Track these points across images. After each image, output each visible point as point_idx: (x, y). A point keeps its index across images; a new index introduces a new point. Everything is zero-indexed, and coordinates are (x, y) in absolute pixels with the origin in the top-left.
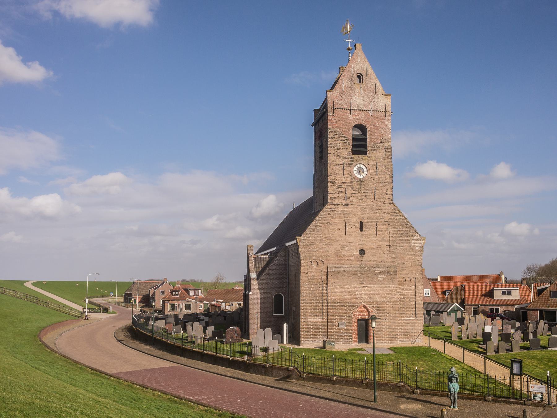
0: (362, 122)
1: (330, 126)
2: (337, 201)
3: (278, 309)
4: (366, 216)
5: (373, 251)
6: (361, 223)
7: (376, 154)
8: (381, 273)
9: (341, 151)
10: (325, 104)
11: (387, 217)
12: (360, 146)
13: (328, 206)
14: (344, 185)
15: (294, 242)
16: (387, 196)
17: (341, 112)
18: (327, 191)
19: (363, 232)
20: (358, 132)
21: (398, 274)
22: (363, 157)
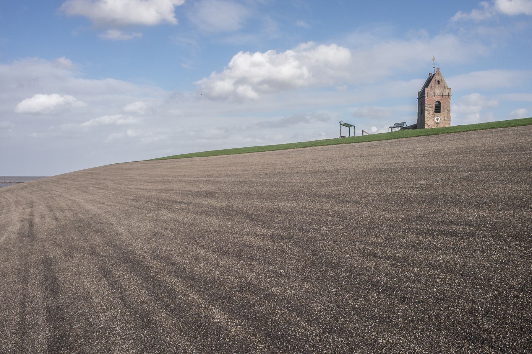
1: (426, 102)
12: (438, 109)
17: (430, 96)
20: (437, 103)
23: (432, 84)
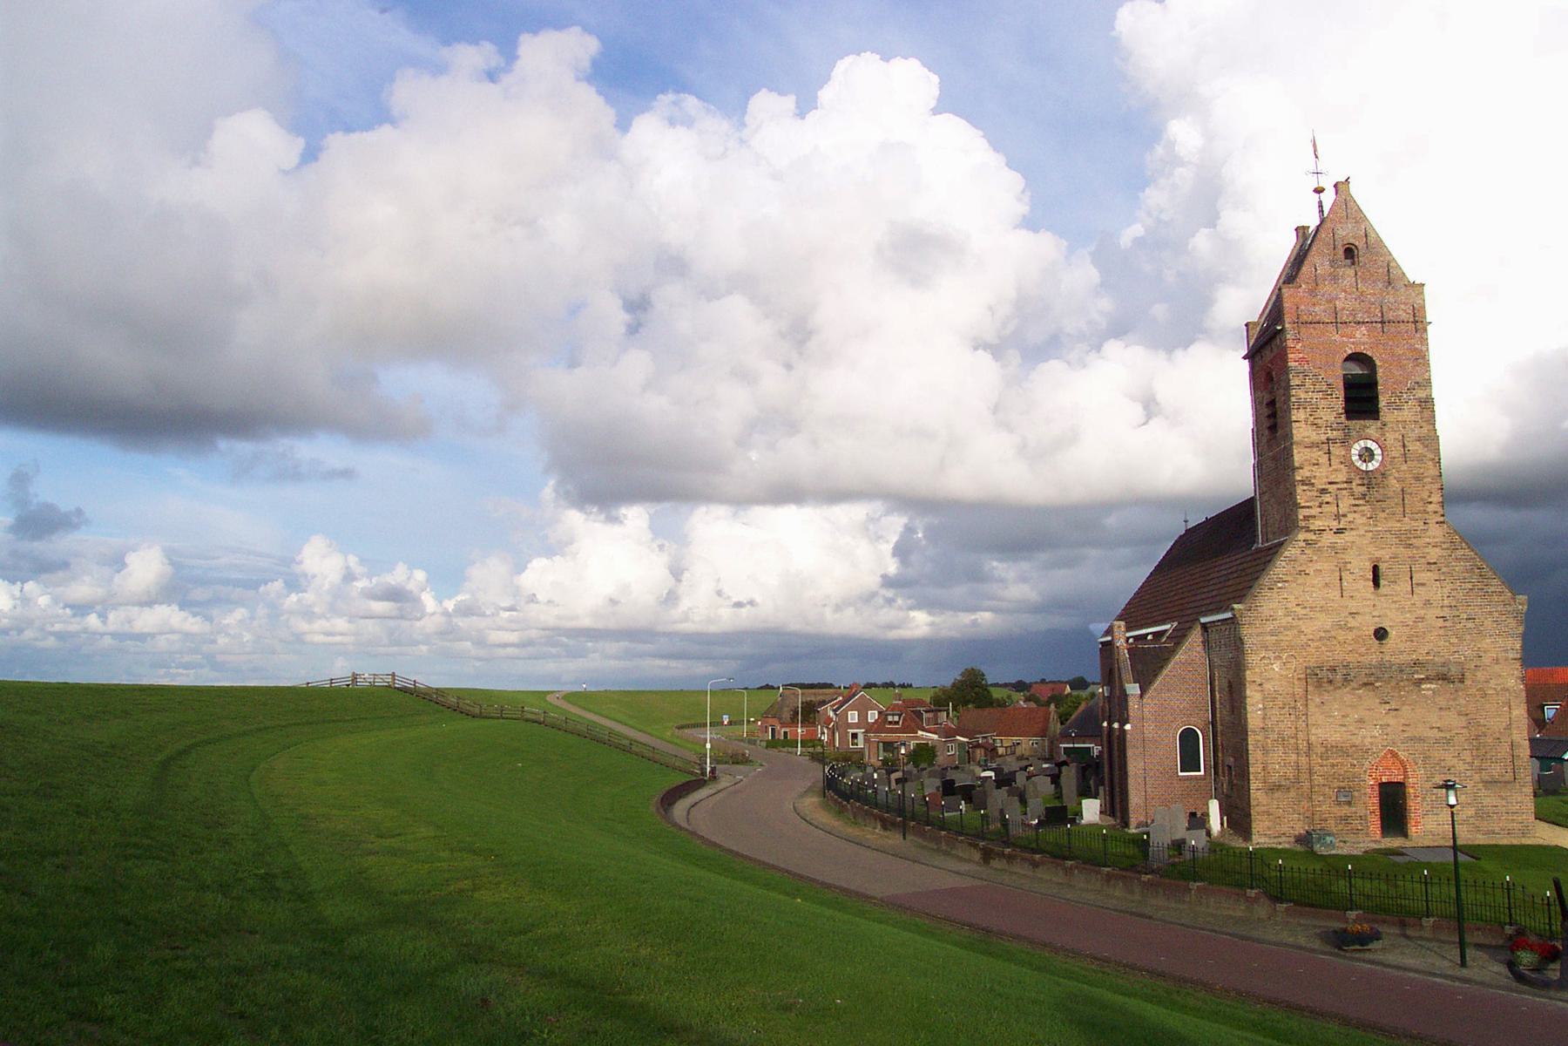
0: (1361, 349)
2: (1317, 524)
3: (1190, 762)
4: (1384, 554)
5: (1406, 630)
6: (1375, 569)
7: (1395, 412)
8: (1428, 679)
9: (1320, 413)
10: (1275, 311)
11: (1434, 554)
12: (1361, 398)
13: (1301, 536)
14: (1331, 488)
15: (1228, 615)
16: (1431, 508)
18: (1297, 506)
19: (1382, 590)
20: (1356, 370)
21: (1468, 682)
22: (1372, 427)
23: (1319, 262)
